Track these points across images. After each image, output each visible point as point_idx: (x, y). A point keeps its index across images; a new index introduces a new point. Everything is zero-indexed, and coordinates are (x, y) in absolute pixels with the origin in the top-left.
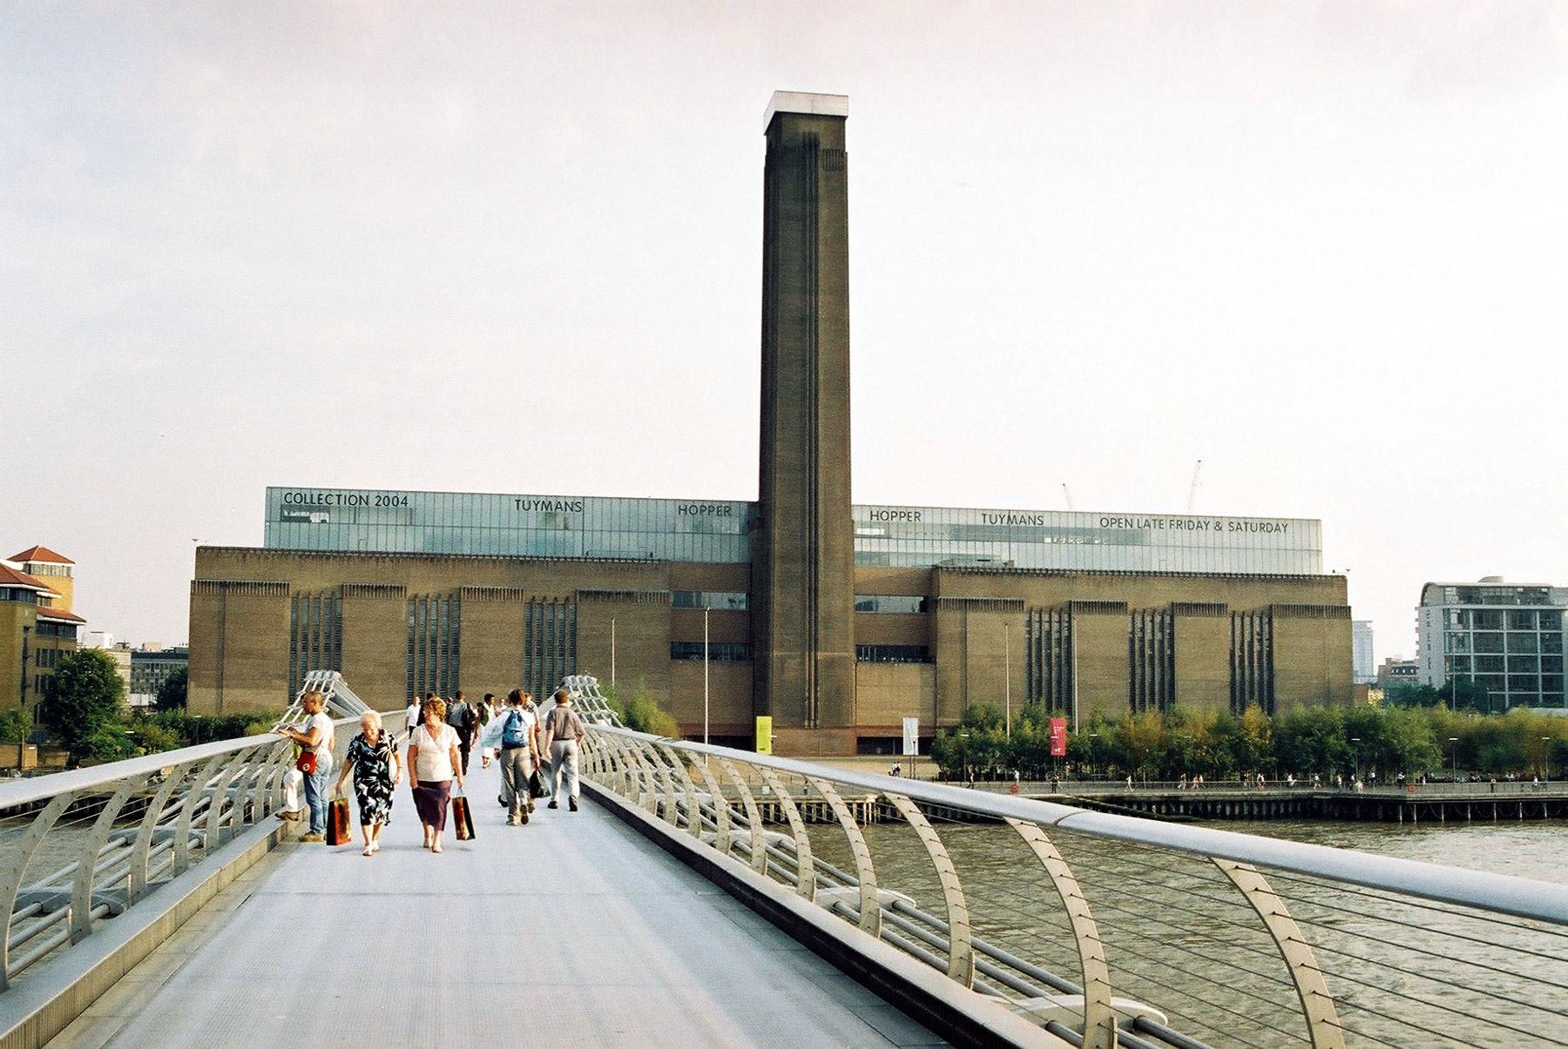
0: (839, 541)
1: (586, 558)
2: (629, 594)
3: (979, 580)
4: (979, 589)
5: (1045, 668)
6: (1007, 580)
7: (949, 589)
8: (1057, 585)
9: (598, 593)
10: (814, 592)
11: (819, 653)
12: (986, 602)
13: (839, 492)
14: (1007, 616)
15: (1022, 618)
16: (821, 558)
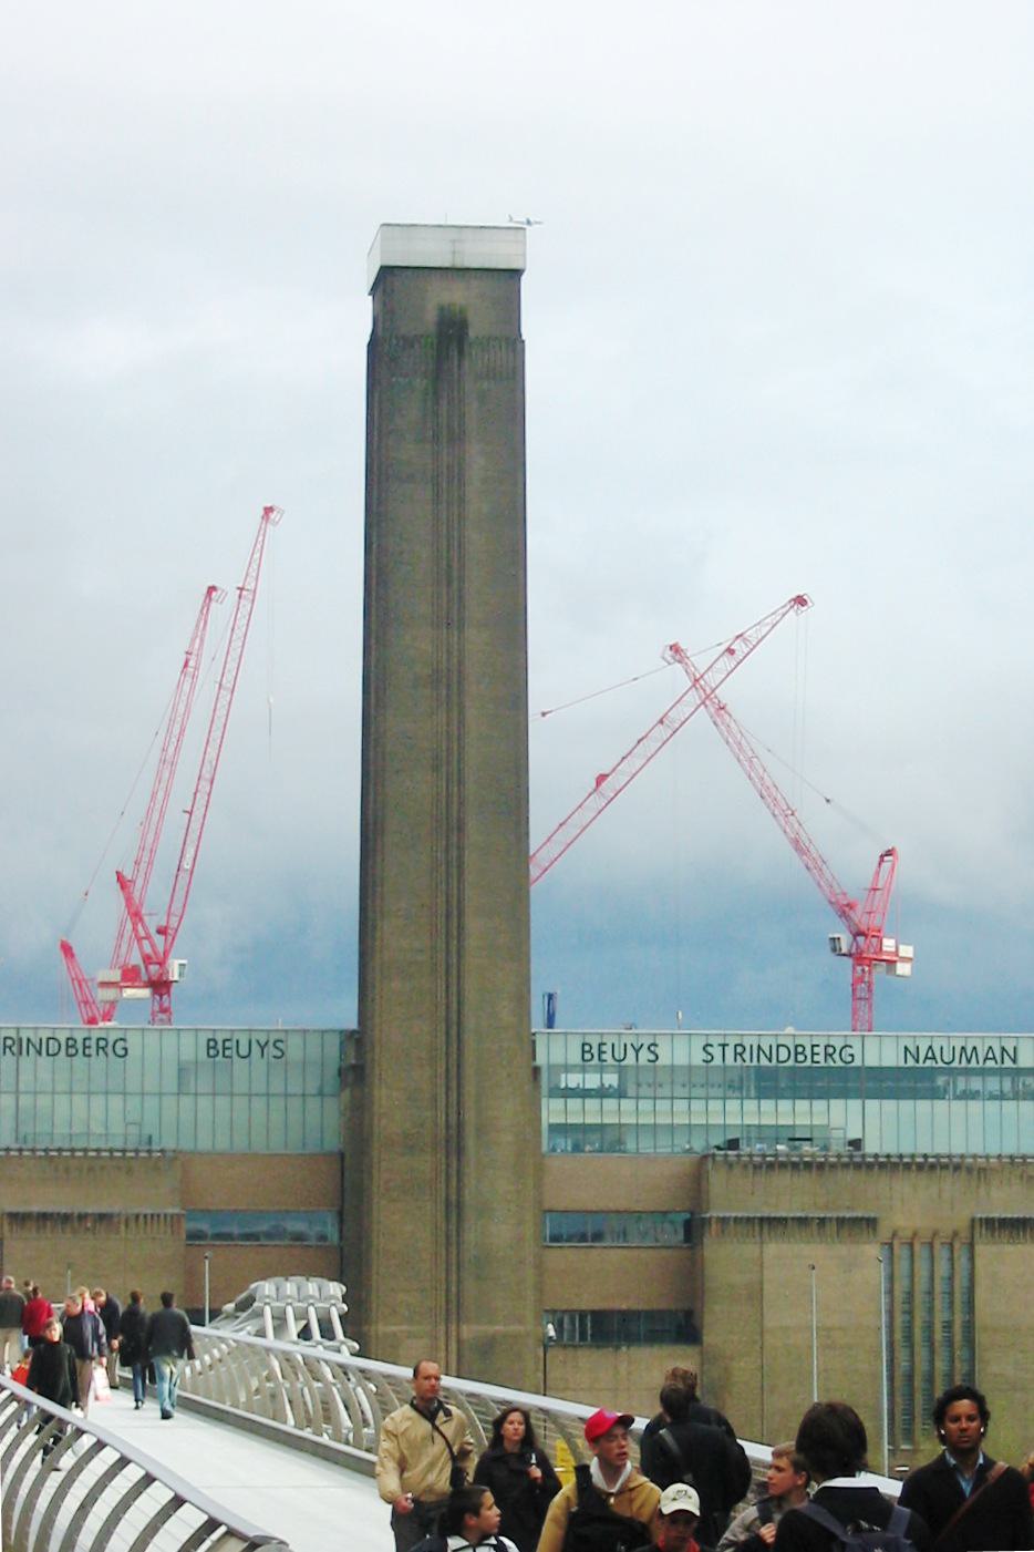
0: (506, 1110)
1: (20, 1150)
2: (102, 1217)
3: (783, 1179)
4: (790, 1197)
5: (921, 1353)
6: (848, 1177)
7: (728, 1197)
8: (949, 1185)
9: (44, 1217)
10: (454, 1209)
11: (464, 1328)
12: (803, 1222)
13: (506, 1015)
14: (842, 1250)
15: (872, 1251)
16: (470, 1142)
